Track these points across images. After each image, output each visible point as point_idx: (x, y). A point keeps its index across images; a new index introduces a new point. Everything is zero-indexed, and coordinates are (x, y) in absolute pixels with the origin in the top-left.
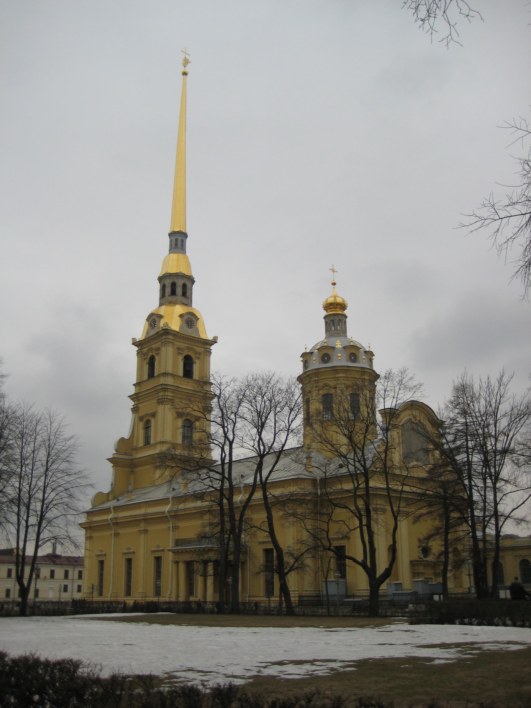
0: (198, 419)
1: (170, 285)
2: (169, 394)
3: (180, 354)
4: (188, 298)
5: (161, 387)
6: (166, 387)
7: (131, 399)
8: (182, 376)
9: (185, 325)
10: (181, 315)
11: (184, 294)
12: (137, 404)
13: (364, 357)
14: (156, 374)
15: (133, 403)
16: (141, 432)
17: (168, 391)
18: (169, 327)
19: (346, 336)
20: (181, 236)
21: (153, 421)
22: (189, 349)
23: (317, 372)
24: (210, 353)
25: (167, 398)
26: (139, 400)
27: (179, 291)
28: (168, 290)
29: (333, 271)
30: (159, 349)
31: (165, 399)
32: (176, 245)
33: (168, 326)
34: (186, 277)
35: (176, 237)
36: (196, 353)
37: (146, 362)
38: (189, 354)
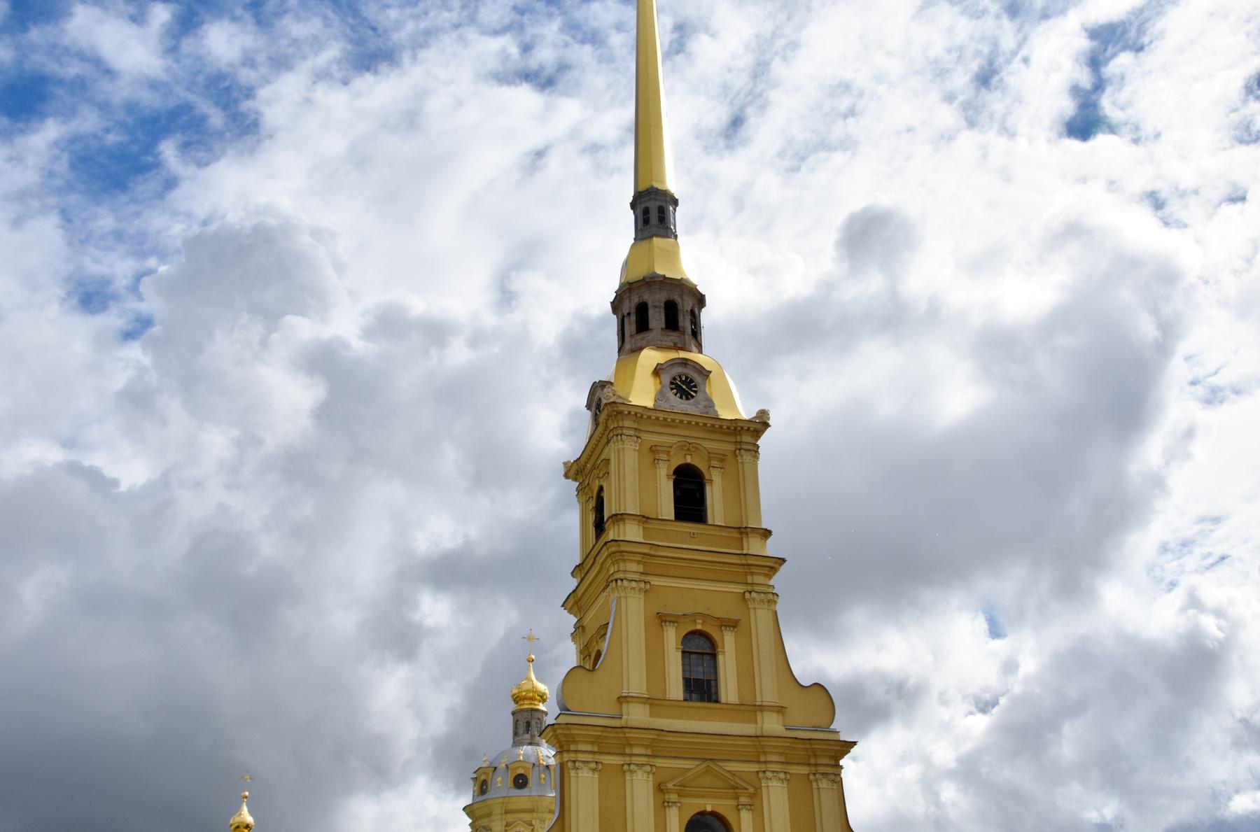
2: (633, 567)
3: (655, 461)
4: (684, 333)
7: (570, 612)
8: (673, 519)
9: (670, 394)
10: (655, 369)
15: (576, 620)
17: (624, 561)
18: (619, 397)
20: (655, 199)
22: (687, 448)
27: (657, 319)
28: (630, 327)
31: (619, 582)
32: (646, 221)
36: (710, 456)
38: (689, 460)
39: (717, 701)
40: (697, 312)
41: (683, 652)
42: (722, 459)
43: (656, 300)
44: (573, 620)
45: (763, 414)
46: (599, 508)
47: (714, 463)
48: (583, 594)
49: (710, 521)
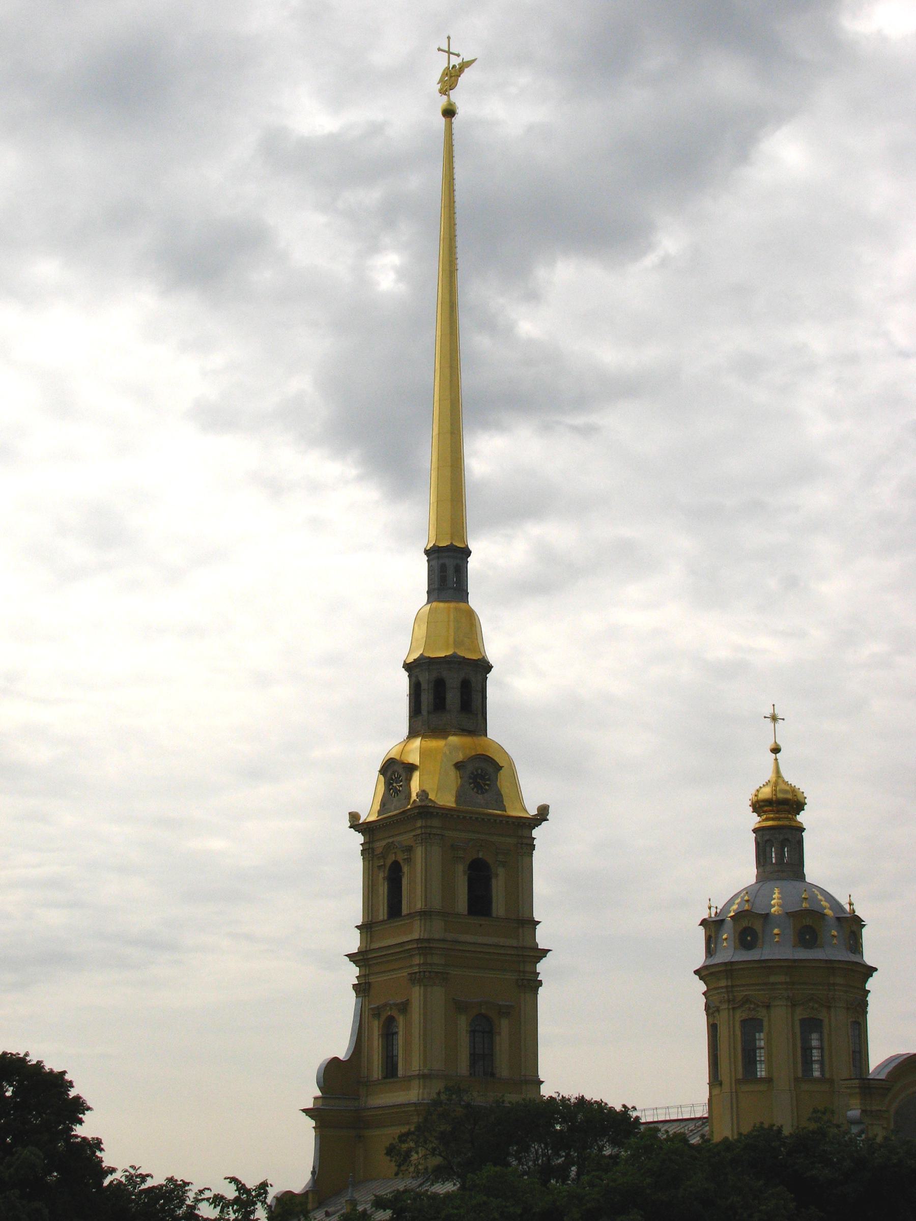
0: (506, 1012)
5: (415, 946)
6: (427, 945)
12: (365, 976)
13: (834, 933)
14: (405, 911)
16: (376, 1043)
19: (801, 876)
21: (401, 1020)
24: (533, 847)
25: (430, 972)
26: (369, 966)
27: (453, 698)
28: (426, 699)
29: (774, 718)
30: (409, 849)
33: (427, 798)
35: (441, 561)
37: (381, 875)
38: (481, 855)
39: (493, 1075)
43: (453, 681)
49: (494, 914)
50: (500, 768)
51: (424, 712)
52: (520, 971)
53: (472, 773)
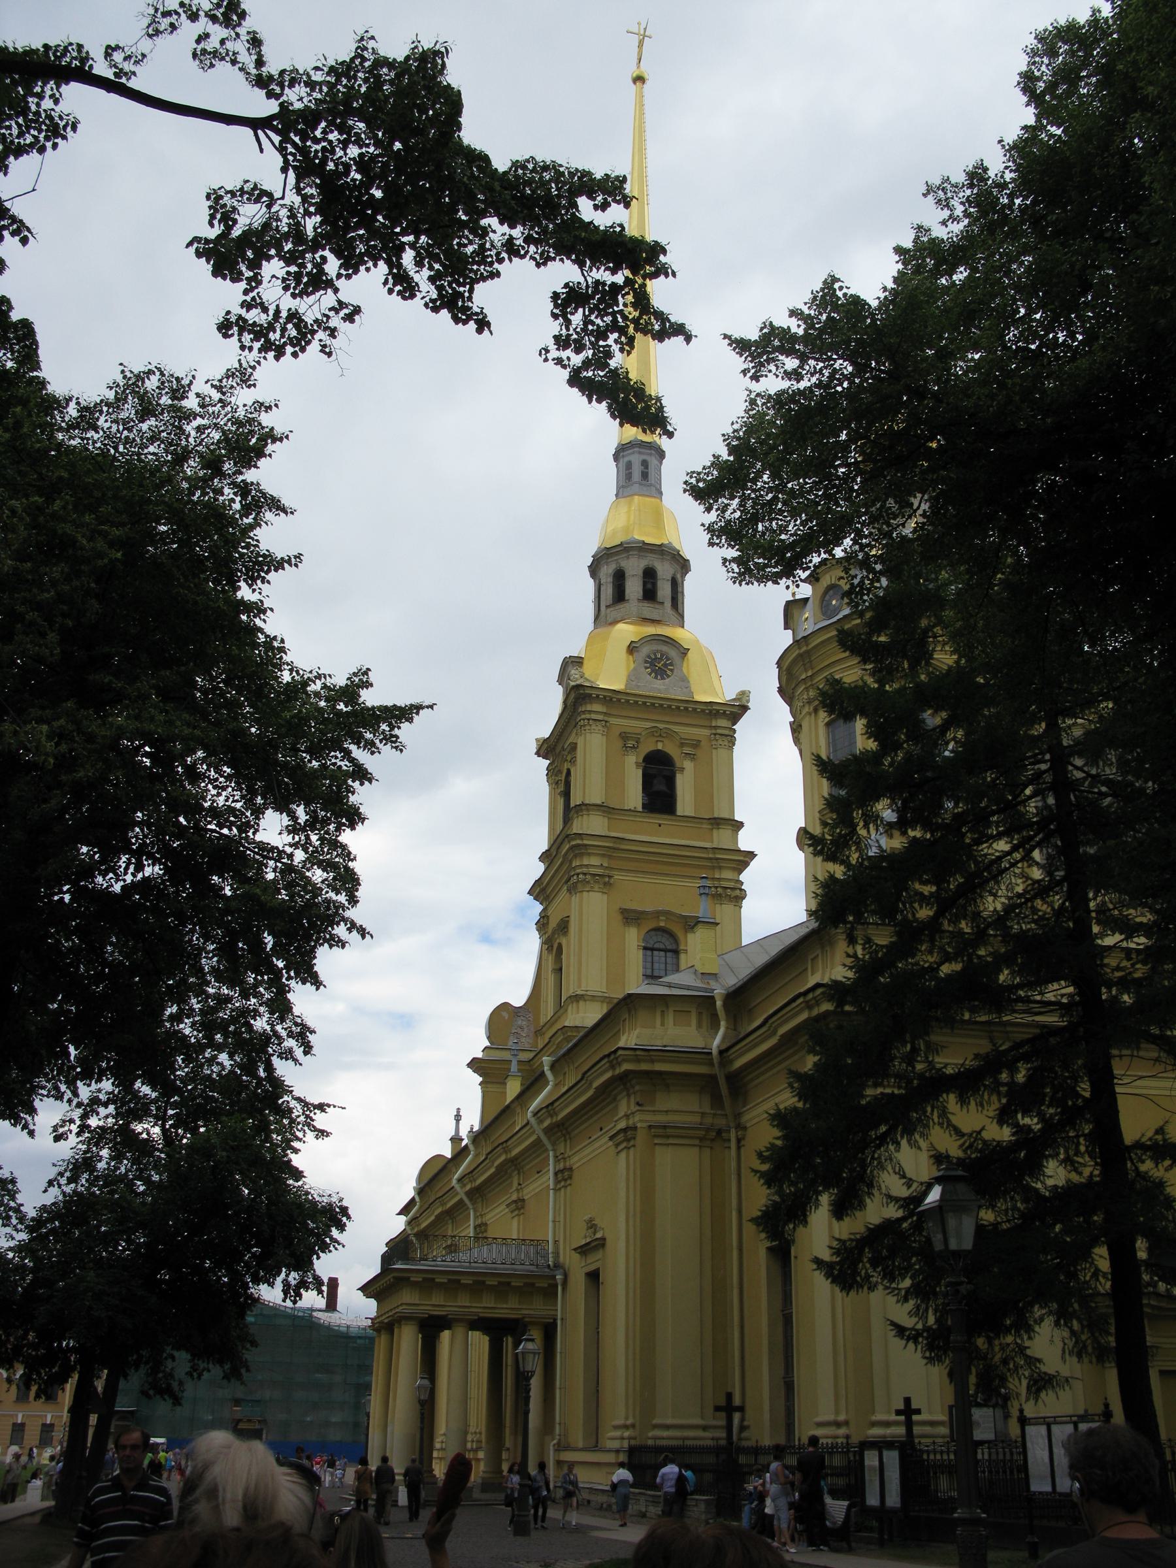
1: (610, 579)
2: (595, 861)
11: (650, 594)
17: (589, 854)
20: (640, 453)
23: (808, 652)
24: (732, 741)
25: (585, 874)
27: (634, 587)
32: (629, 476)
34: (652, 551)
35: (626, 459)
38: (660, 746)
40: (679, 576)
41: (645, 948)
42: (696, 744)
43: (634, 568)
44: (539, 908)
45: (744, 695)
46: (566, 794)
47: (687, 750)
48: (548, 884)
49: (679, 812)
50: (684, 652)
51: (603, 608)
52: (713, 879)
53: (649, 657)
